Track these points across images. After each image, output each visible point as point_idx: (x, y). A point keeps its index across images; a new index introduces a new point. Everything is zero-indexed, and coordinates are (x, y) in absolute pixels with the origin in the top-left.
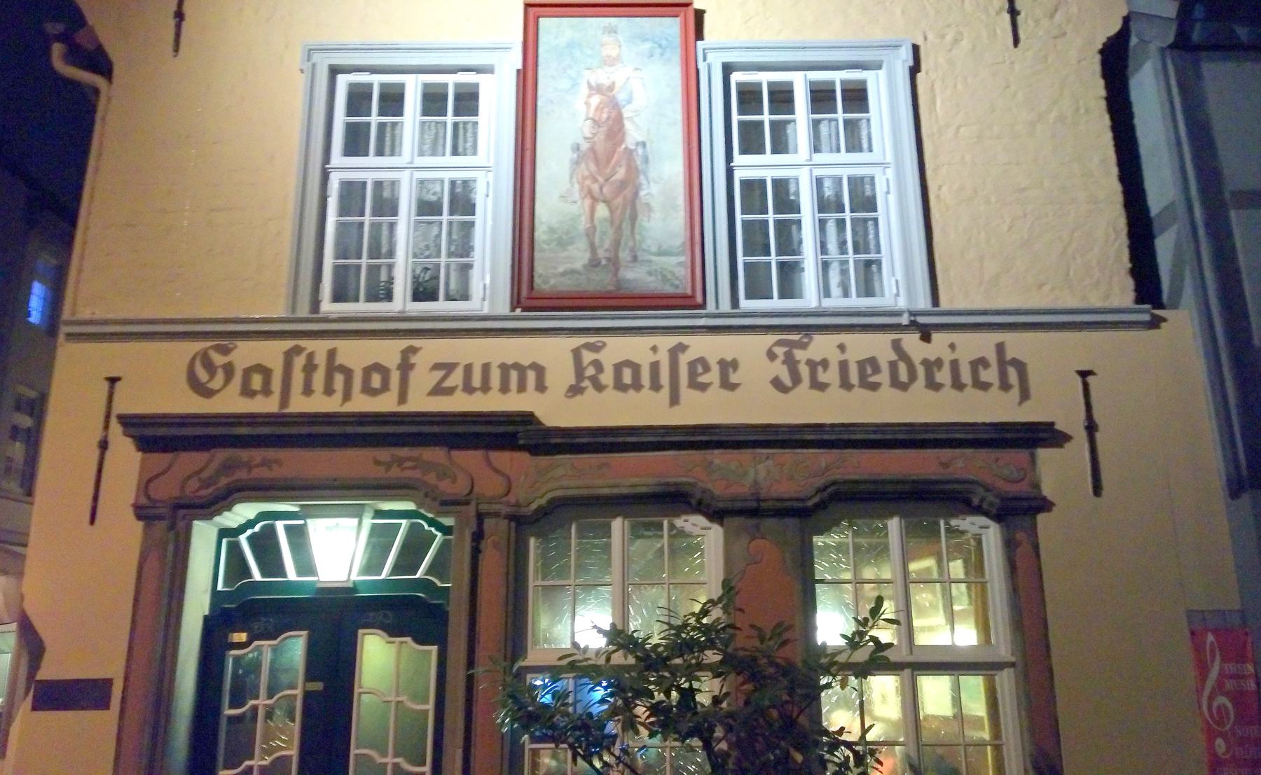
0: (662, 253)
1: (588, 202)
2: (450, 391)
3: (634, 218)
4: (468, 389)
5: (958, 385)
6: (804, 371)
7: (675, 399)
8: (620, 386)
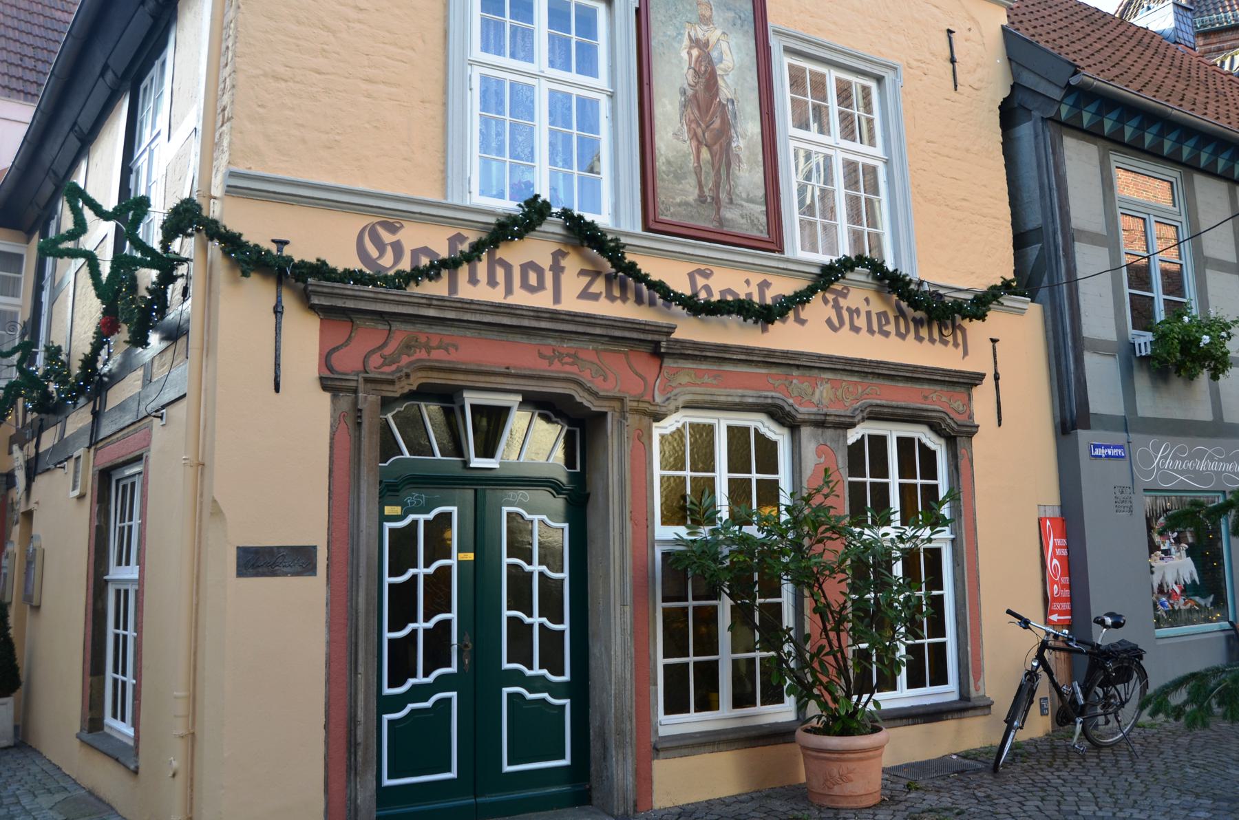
0: (750, 200)
1: (694, 143)
6: (846, 315)
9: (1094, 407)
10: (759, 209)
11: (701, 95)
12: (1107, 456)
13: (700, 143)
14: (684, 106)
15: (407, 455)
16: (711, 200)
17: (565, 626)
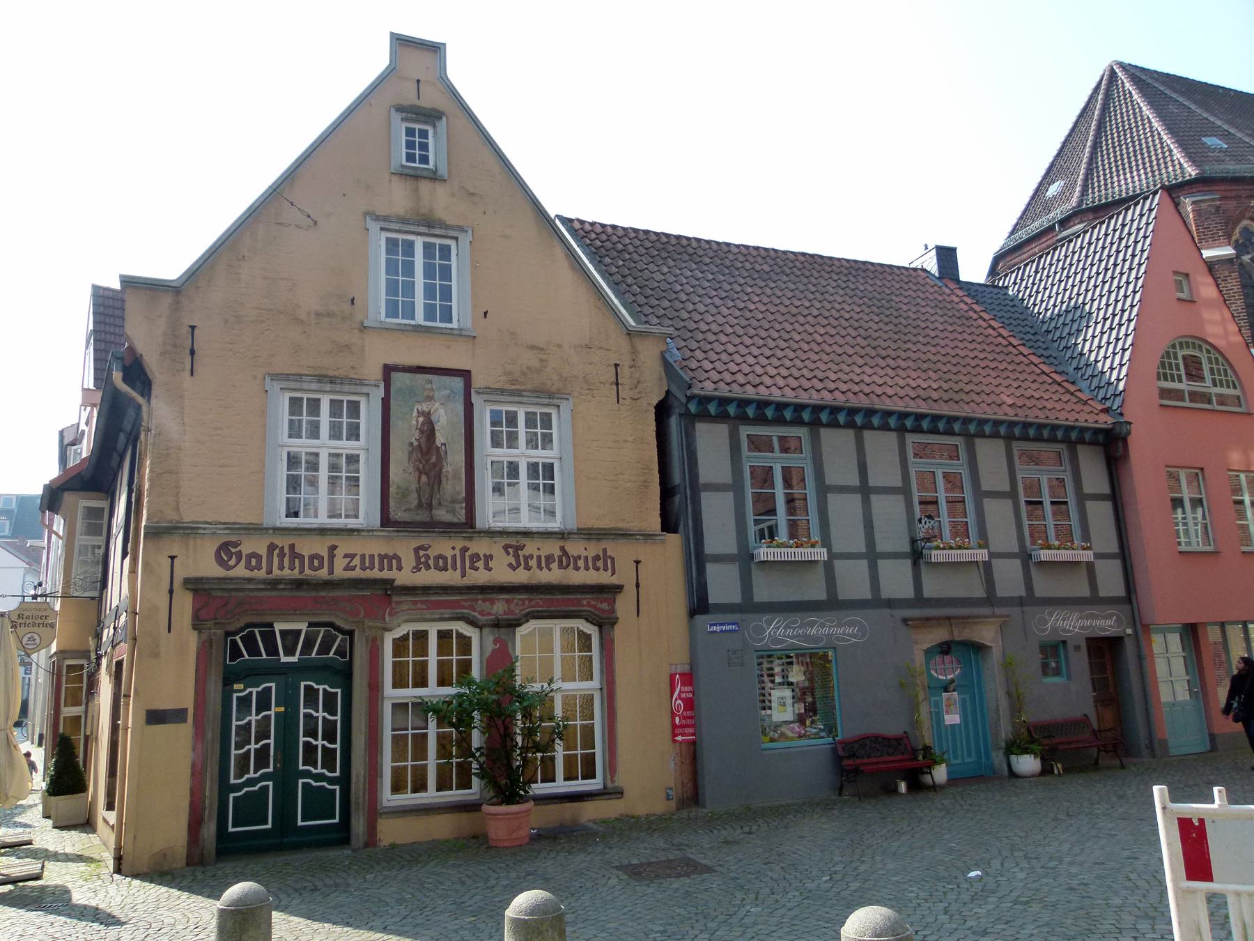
2: (354, 568)
5: (587, 568)
6: (522, 559)
9: (711, 600)
11: (423, 445)
12: (722, 631)
13: (421, 473)
14: (411, 453)
16: (426, 505)
17: (338, 746)
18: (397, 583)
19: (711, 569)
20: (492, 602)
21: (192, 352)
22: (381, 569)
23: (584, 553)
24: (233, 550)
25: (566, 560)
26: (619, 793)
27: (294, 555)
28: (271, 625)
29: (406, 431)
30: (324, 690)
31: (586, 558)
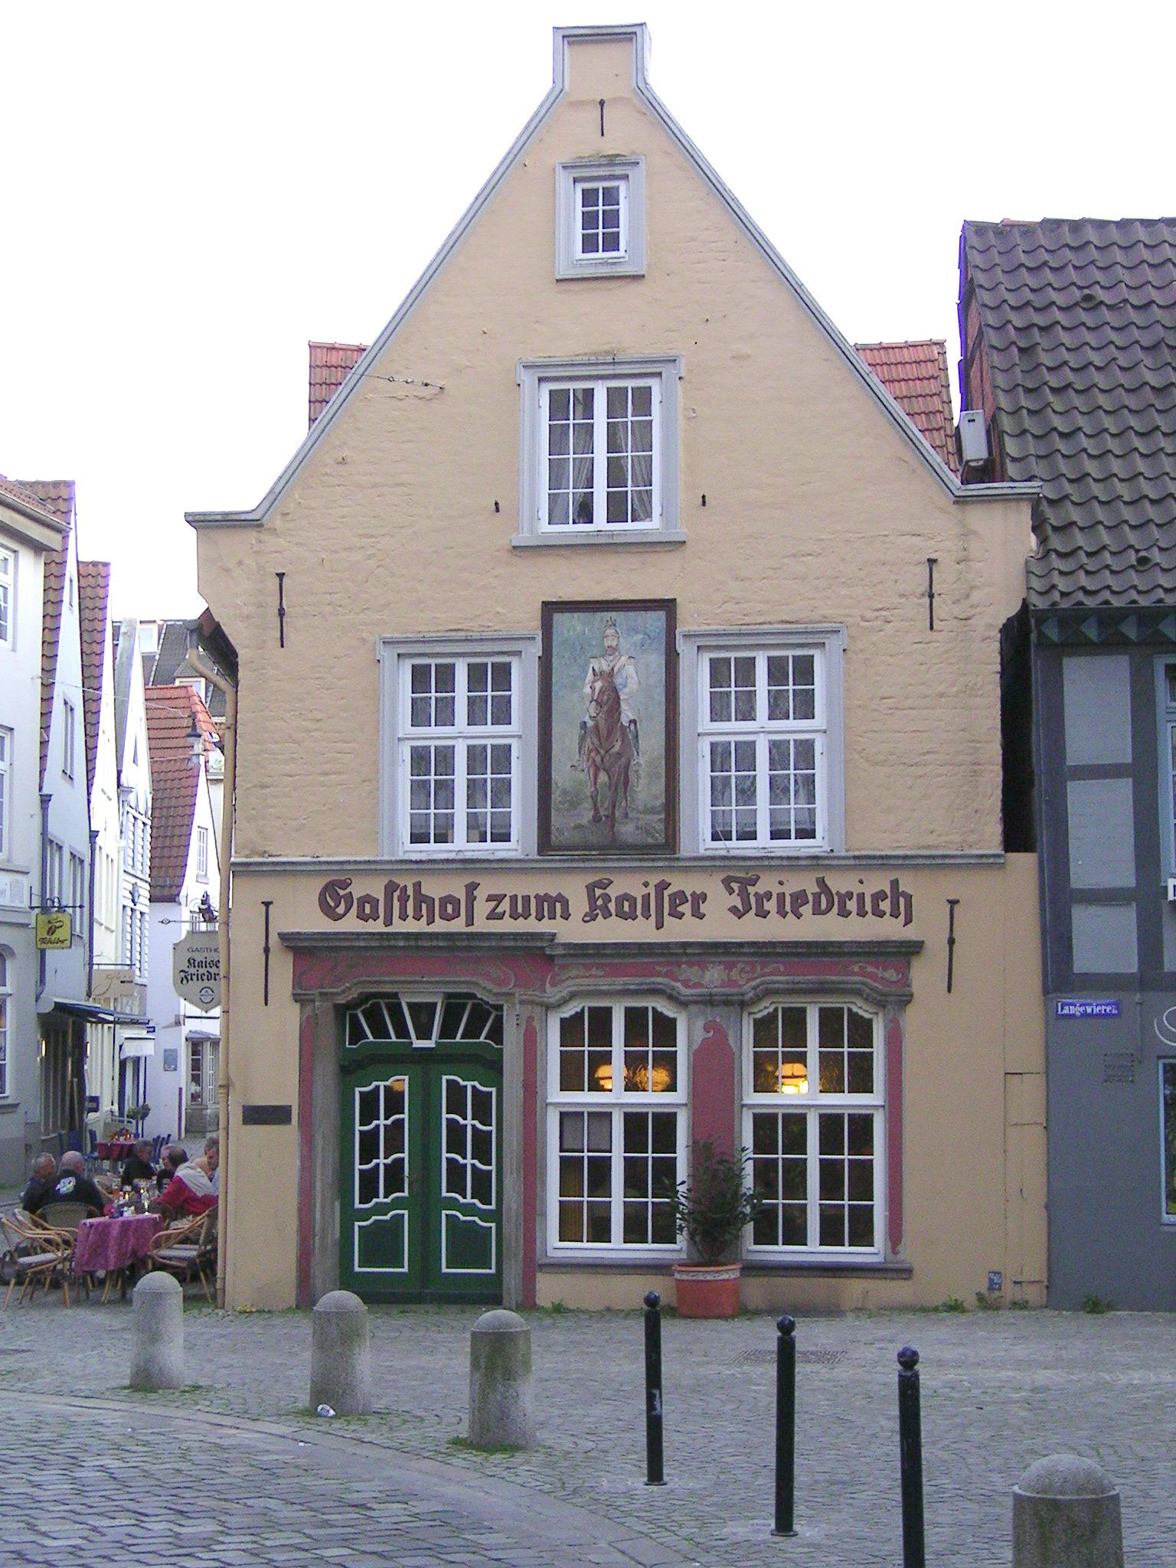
2: (501, 917)
3: (626, 783)
4: (514, 916)
5: (862, 913)
7: (659, 925)
8: (621, 915)
10: (657, 821)
14: (582, 739)
15: (371, 1038)
18: (560, 940)
19: (1082, 918)
20: (703, 967)
21: (281, 613)
22: (540, 918)
23: (857, 889)
24: (342, 892)
25: (827, 901)
26: (905, 1273)
27: (421, 899)
28: (395, 995)
29: (576, 705)
30: (474, 1087)
31: (861, 897)
